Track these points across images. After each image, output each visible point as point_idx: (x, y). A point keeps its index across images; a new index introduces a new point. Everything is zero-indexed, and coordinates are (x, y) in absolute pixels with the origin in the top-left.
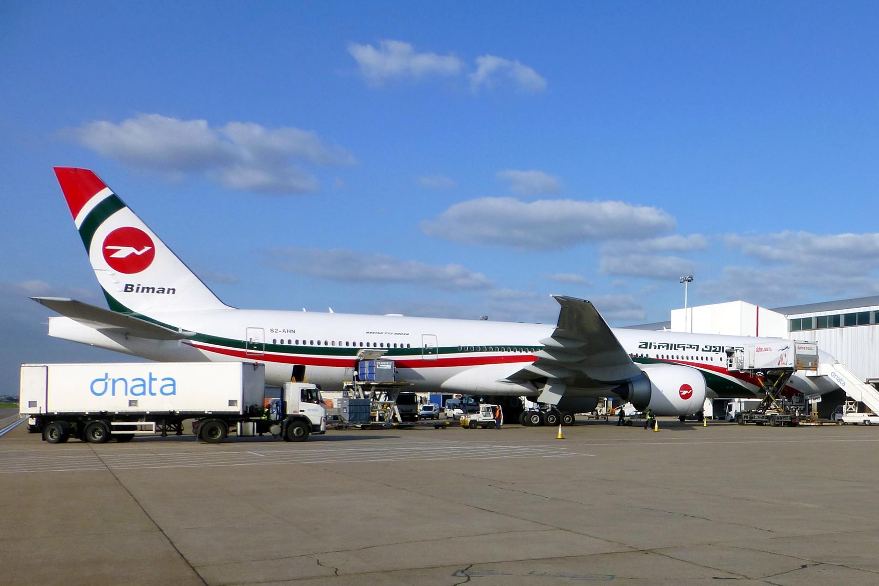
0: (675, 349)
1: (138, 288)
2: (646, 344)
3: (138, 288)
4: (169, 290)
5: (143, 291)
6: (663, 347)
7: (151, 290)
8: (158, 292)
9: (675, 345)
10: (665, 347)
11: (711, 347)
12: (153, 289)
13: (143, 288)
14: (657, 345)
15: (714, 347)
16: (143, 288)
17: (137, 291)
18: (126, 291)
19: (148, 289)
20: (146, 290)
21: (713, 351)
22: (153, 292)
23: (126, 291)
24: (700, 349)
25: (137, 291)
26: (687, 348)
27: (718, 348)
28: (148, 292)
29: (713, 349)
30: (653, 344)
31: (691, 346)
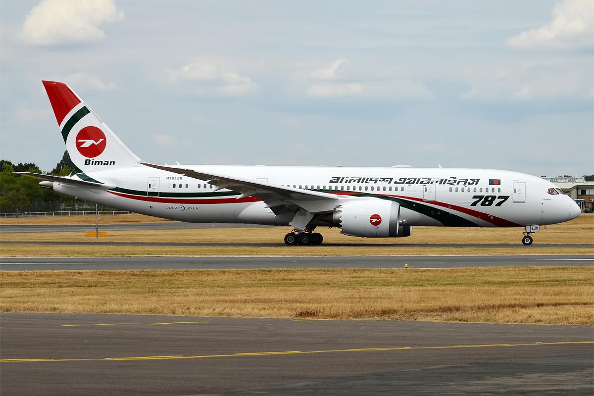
0: (366, 182)
1: (93, 162)
2: (338, 179)
3: (93, 162)
4: (111, 162)
5: (95, 164)
6: (354, 181)
7: (100, 163)
8: (104, 164)
9: (368, 178)
10: (357, 181)
11: (405, 179)
12: (102, 162)
13: (96, 162)
14: (349, 180)
15: (409, 179)
16: (96, 162)
17: (92, 164)
18: (86, 164)
19: (99, 162)
20: (97, 163)
21: (406, 183)
22: (101, 164)
23: (86, 164)
24: (393, 181)
25: (92, 164)
26: (380, 181)
27: (413, 180)
28: (98, 164)
29: (407, 181)
30: (345, 179)
31: (384, 180)
